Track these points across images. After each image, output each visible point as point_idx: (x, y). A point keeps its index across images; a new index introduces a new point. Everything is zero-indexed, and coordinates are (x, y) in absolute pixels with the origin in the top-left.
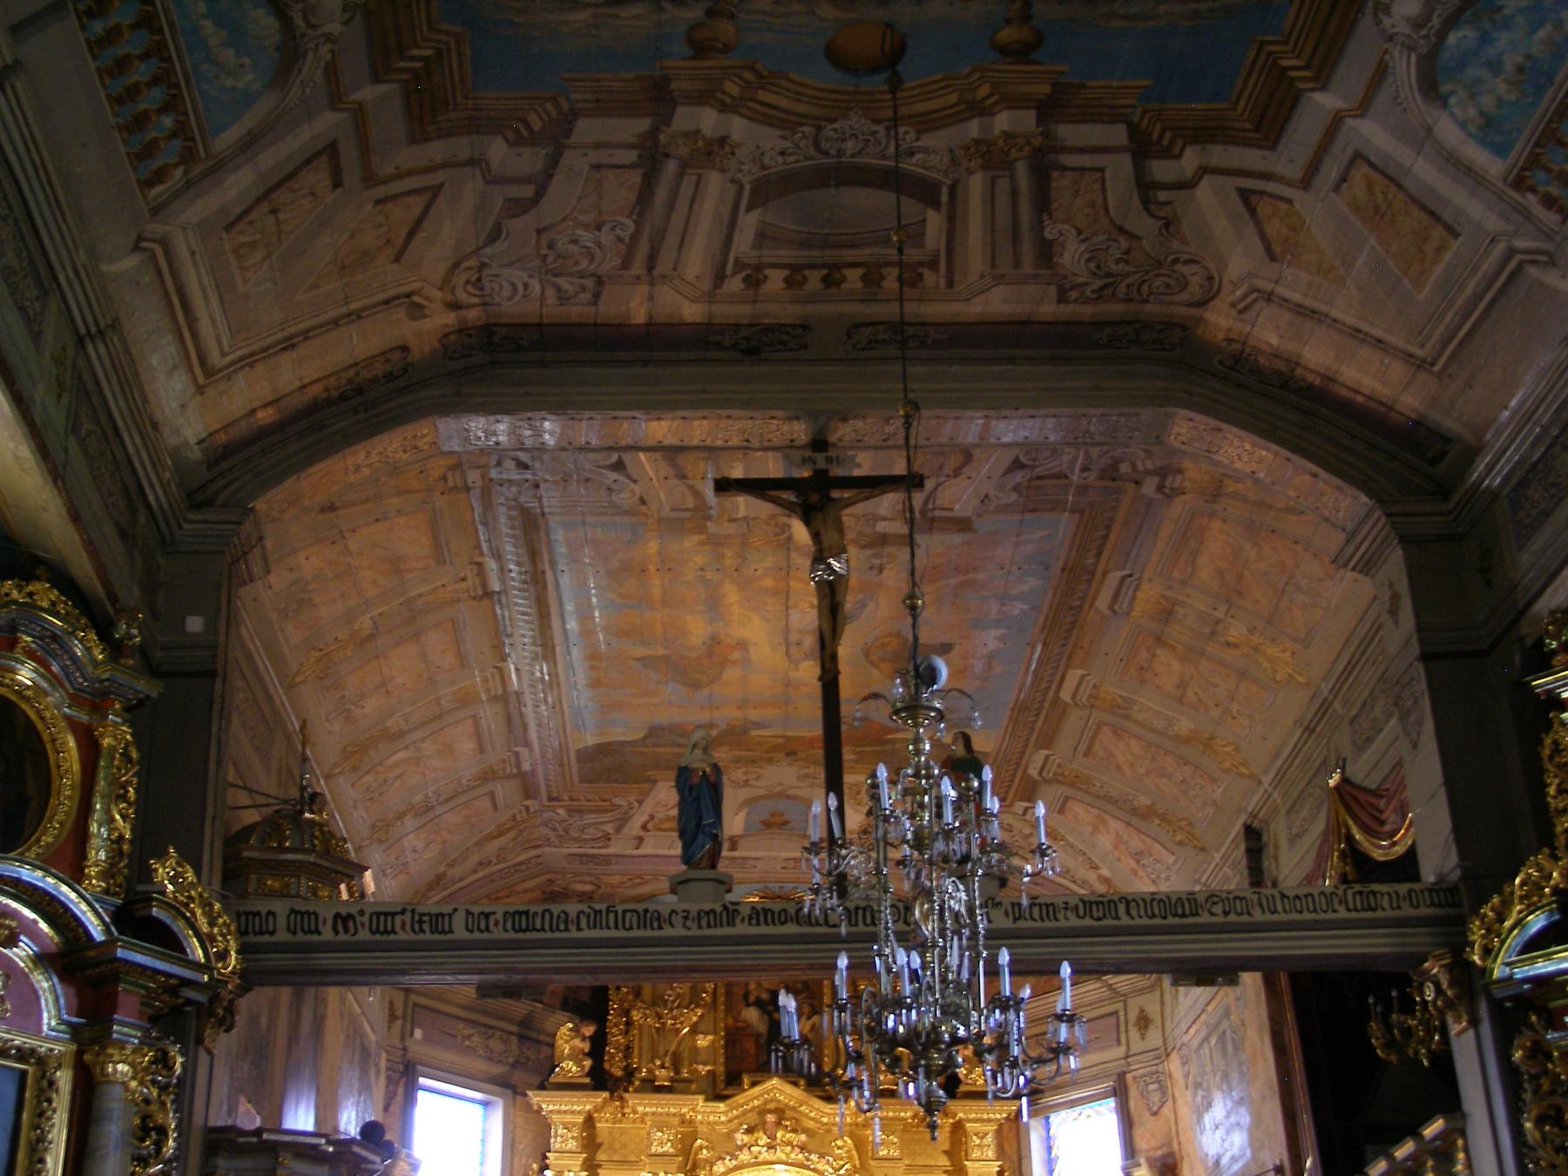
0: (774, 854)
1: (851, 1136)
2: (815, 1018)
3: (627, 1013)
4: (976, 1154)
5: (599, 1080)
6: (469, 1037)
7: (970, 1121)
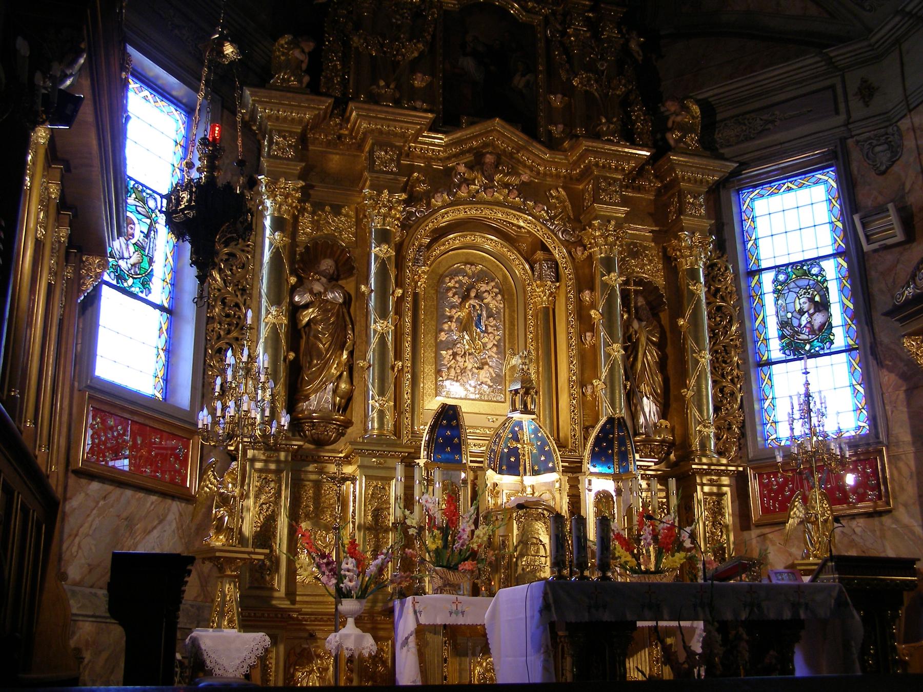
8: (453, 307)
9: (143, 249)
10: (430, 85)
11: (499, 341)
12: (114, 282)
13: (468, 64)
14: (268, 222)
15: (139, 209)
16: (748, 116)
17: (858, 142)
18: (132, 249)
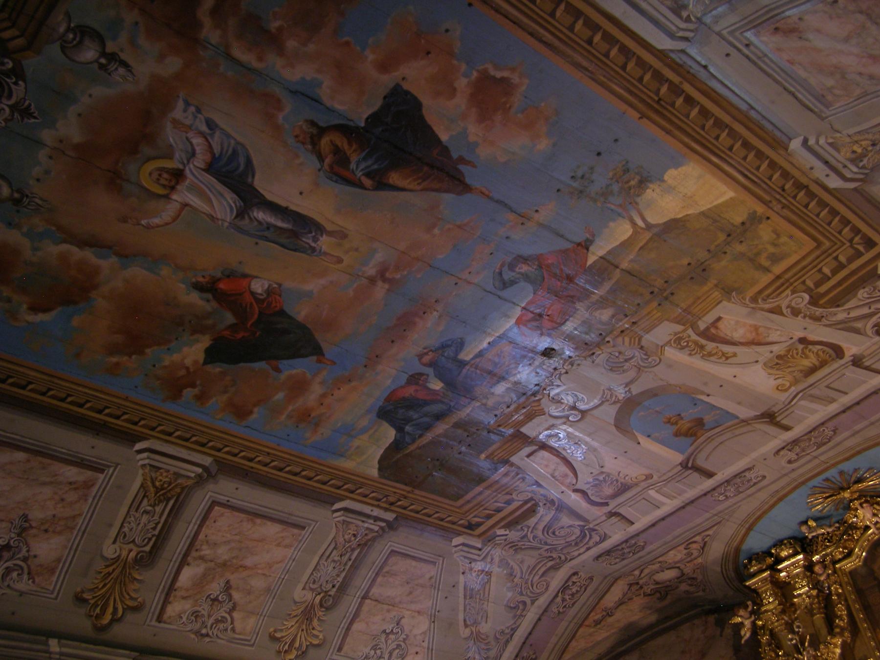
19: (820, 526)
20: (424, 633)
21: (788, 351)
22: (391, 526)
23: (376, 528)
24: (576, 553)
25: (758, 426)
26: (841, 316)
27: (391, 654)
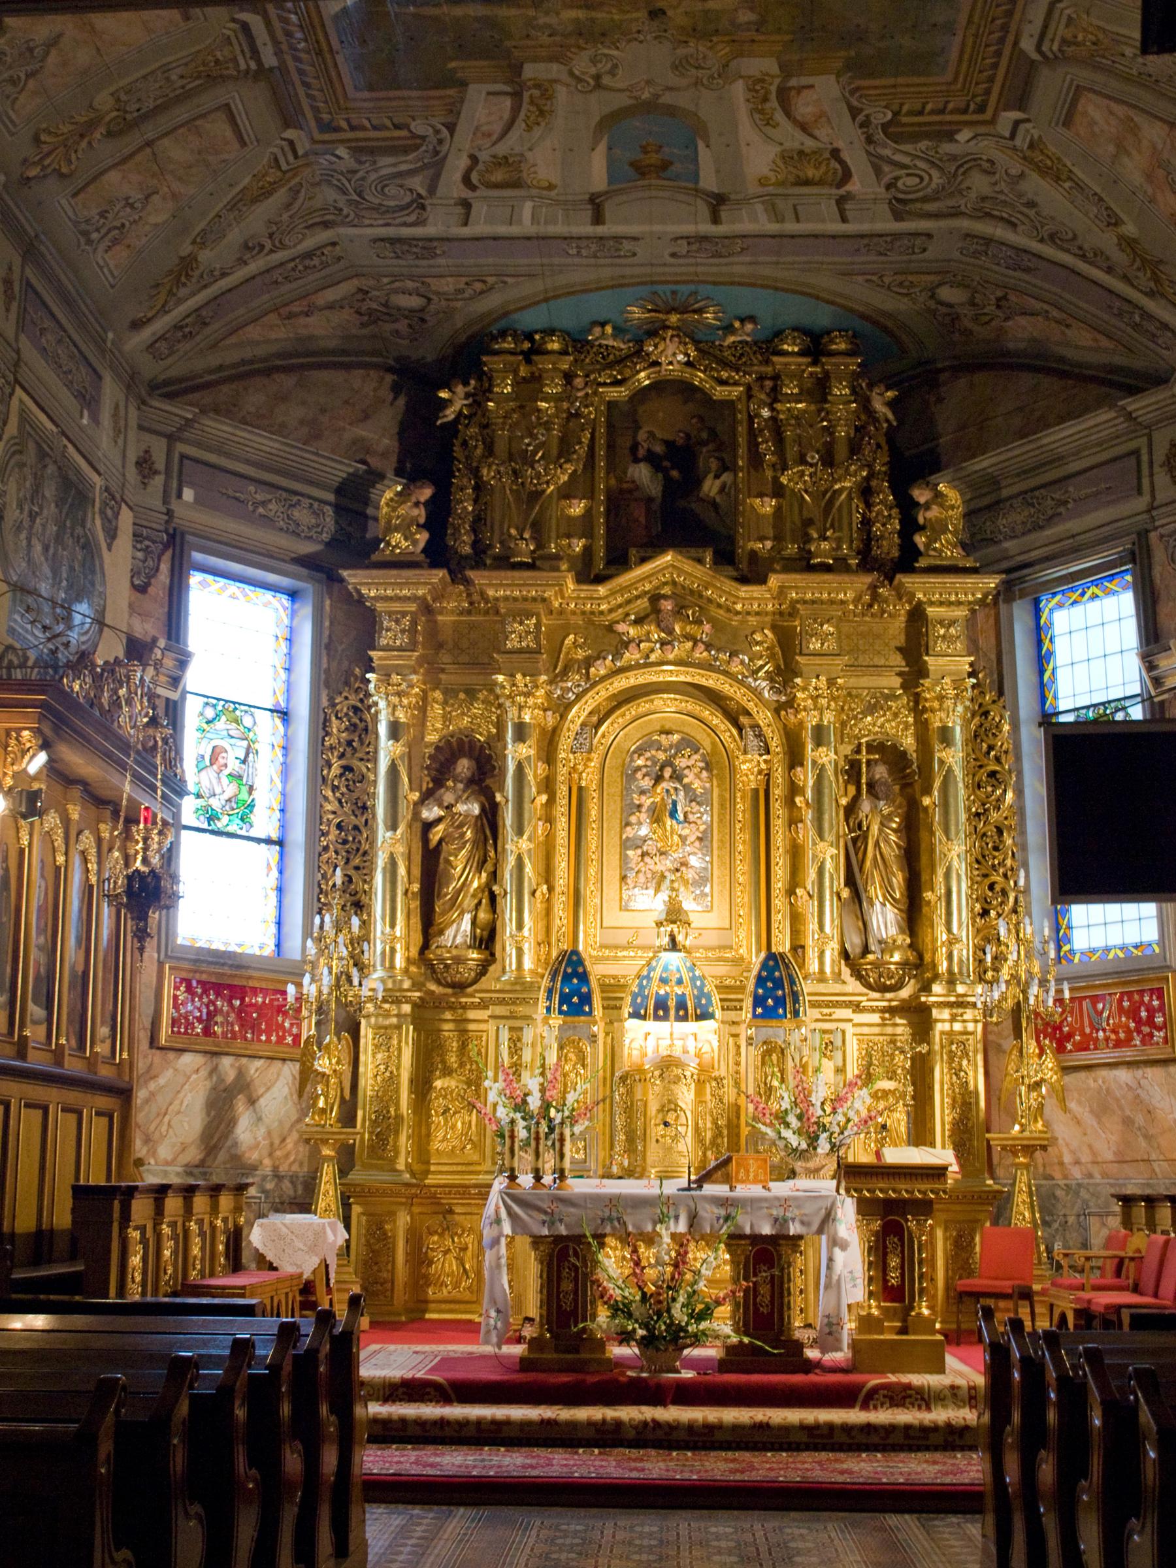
0: (657, 228)
1: (774, 628)
2: (726, 477)
3: (476, 473)
4: (940, 646)
5: (437, 554)
6: (264, 504)
7: (932, 603)
8: (643, 792)
9: (240, 777)
10: (588, 512)
11: (704, 832)
12: (205, 826)
13: (642, 473)
14: (383, 729)
15: (232, 733)
16: (1037, 493)
17: (1162, 536)
18: (225, 781)
19: (614, 336)
20: (156, 225)
21: (814, 153)
22: (261, 73)
23: (243, 66)
24: (367, 222)
25: (699, 201)
26: (887, 152)
27: (109, 231)
